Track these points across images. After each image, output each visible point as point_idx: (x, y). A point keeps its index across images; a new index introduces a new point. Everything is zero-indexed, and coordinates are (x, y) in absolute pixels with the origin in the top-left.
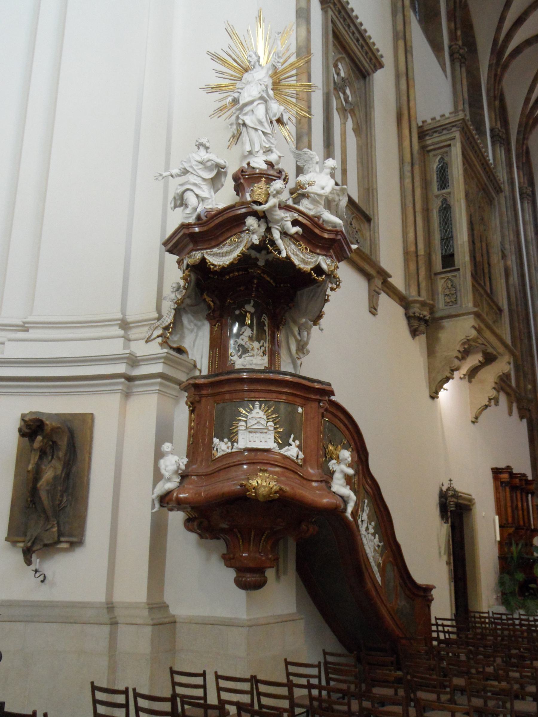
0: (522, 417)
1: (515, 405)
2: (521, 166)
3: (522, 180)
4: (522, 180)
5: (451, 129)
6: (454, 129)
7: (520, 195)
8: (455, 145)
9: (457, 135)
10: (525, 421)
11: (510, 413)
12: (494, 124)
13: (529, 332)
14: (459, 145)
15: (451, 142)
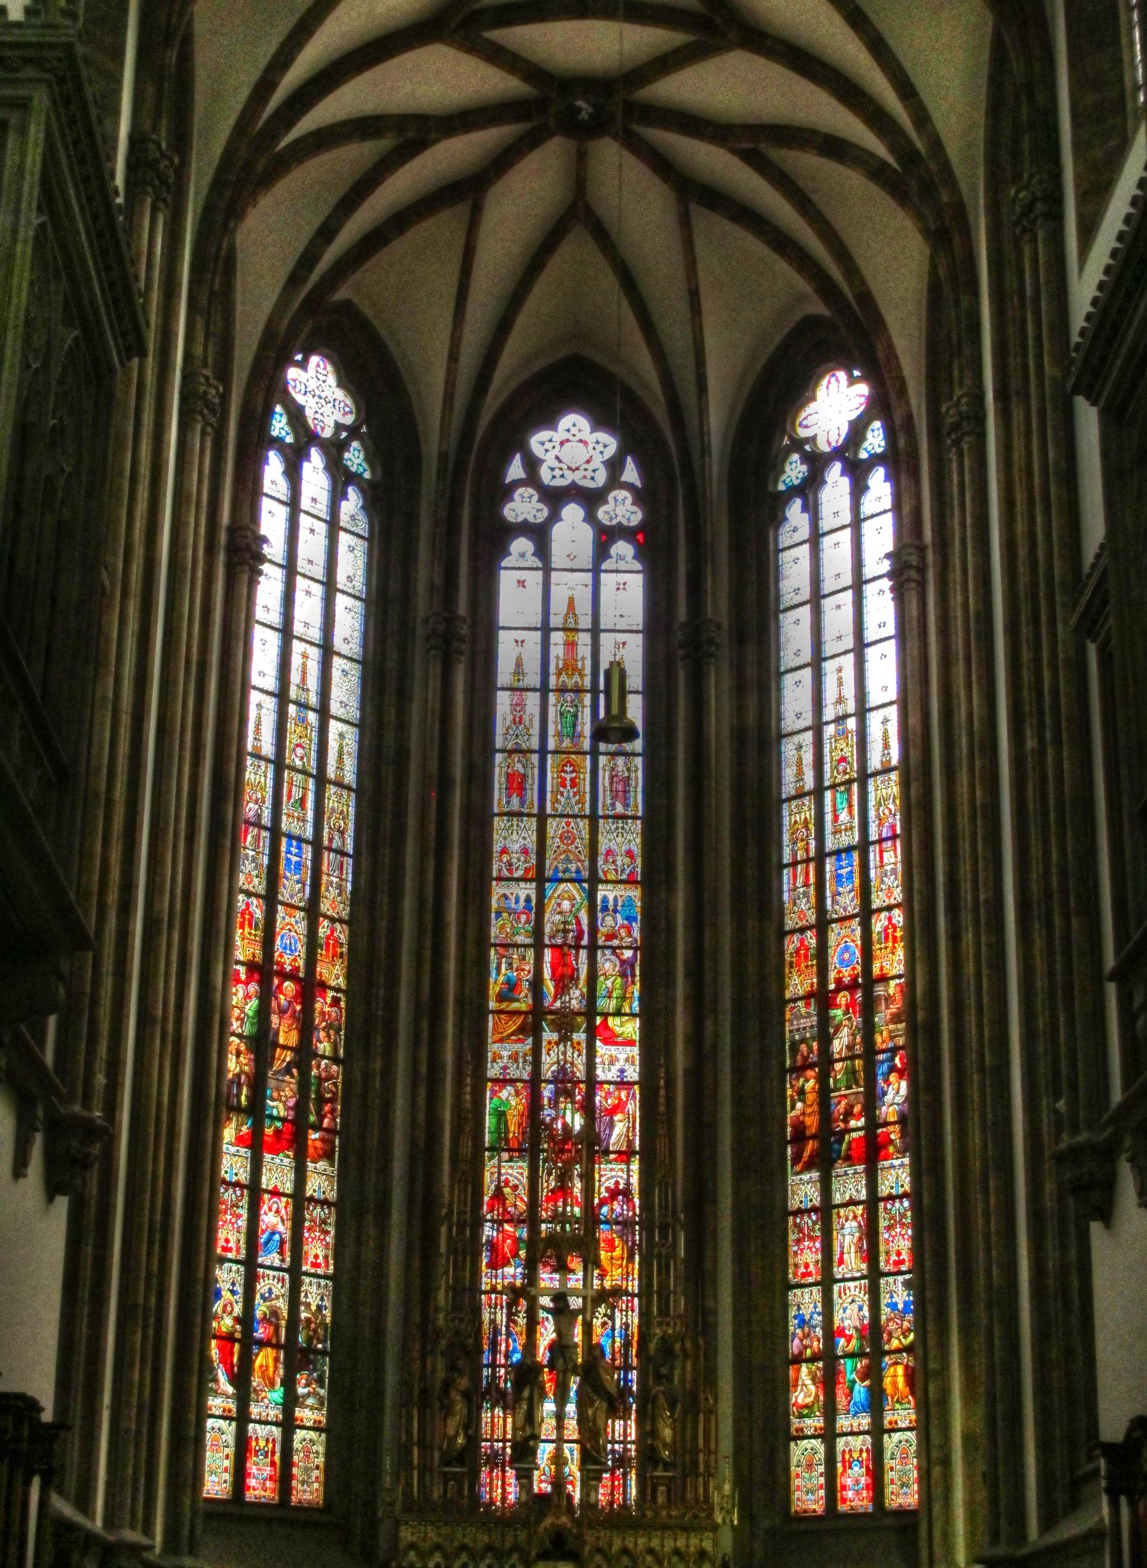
0: (52, 1189)
1: (39, 1140)
2: (204, 302)
3: (199, 350)
4: (199, 350)
5: (17, 70)
6: (29, 72)
7: (183, 399)
8: (23, 131)
9: (40, 99)
10: (62, 1203)
11: (19, 1169)
12: (147, 125)
13: (128, 887)
14: (36, 132)
15: (14, 118)
